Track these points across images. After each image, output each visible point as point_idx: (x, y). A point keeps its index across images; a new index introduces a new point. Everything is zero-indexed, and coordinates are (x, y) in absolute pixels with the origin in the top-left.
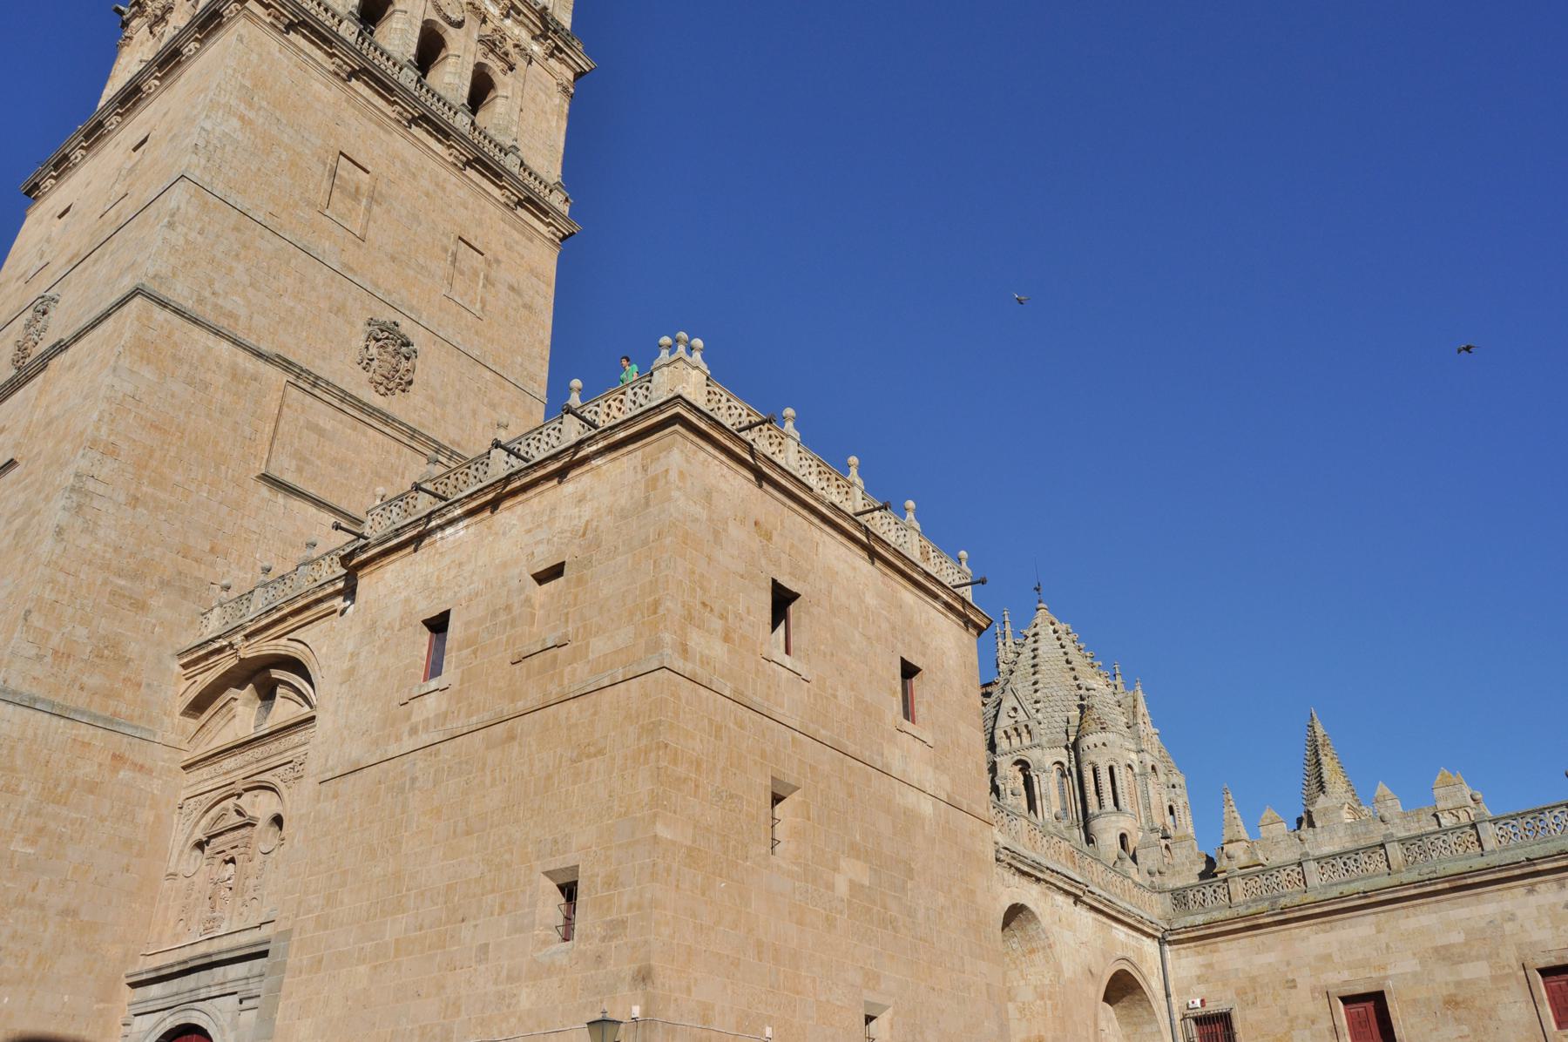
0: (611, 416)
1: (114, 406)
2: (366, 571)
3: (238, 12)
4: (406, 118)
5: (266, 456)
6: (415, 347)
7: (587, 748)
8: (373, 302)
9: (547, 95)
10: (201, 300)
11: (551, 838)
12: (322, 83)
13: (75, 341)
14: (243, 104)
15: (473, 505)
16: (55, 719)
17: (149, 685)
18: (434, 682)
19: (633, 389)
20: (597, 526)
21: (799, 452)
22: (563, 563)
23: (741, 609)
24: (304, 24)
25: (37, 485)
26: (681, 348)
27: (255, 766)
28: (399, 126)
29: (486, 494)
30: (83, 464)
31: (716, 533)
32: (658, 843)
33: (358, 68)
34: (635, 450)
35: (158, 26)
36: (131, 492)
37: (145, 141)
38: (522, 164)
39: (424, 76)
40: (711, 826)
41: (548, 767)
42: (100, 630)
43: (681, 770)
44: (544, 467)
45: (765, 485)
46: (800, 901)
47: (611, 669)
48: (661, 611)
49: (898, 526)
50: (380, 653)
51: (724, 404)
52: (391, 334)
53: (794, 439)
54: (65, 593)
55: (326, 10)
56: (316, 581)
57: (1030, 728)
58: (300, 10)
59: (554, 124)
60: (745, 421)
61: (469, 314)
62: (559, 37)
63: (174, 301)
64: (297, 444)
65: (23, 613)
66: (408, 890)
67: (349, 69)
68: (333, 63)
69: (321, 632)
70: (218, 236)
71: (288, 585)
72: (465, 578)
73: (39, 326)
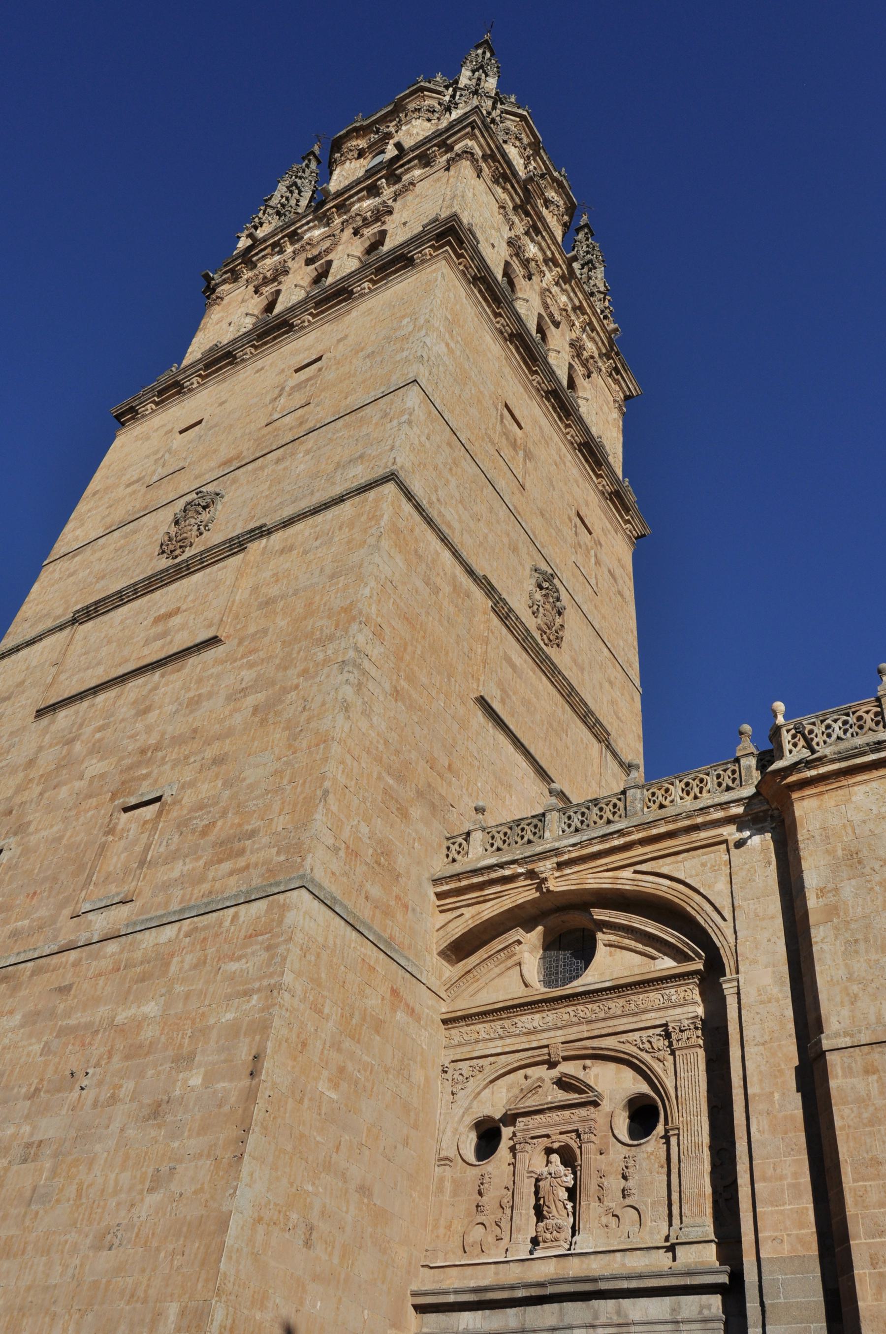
13: (284, 527)
17: (414, 910)
37: (319, 359)
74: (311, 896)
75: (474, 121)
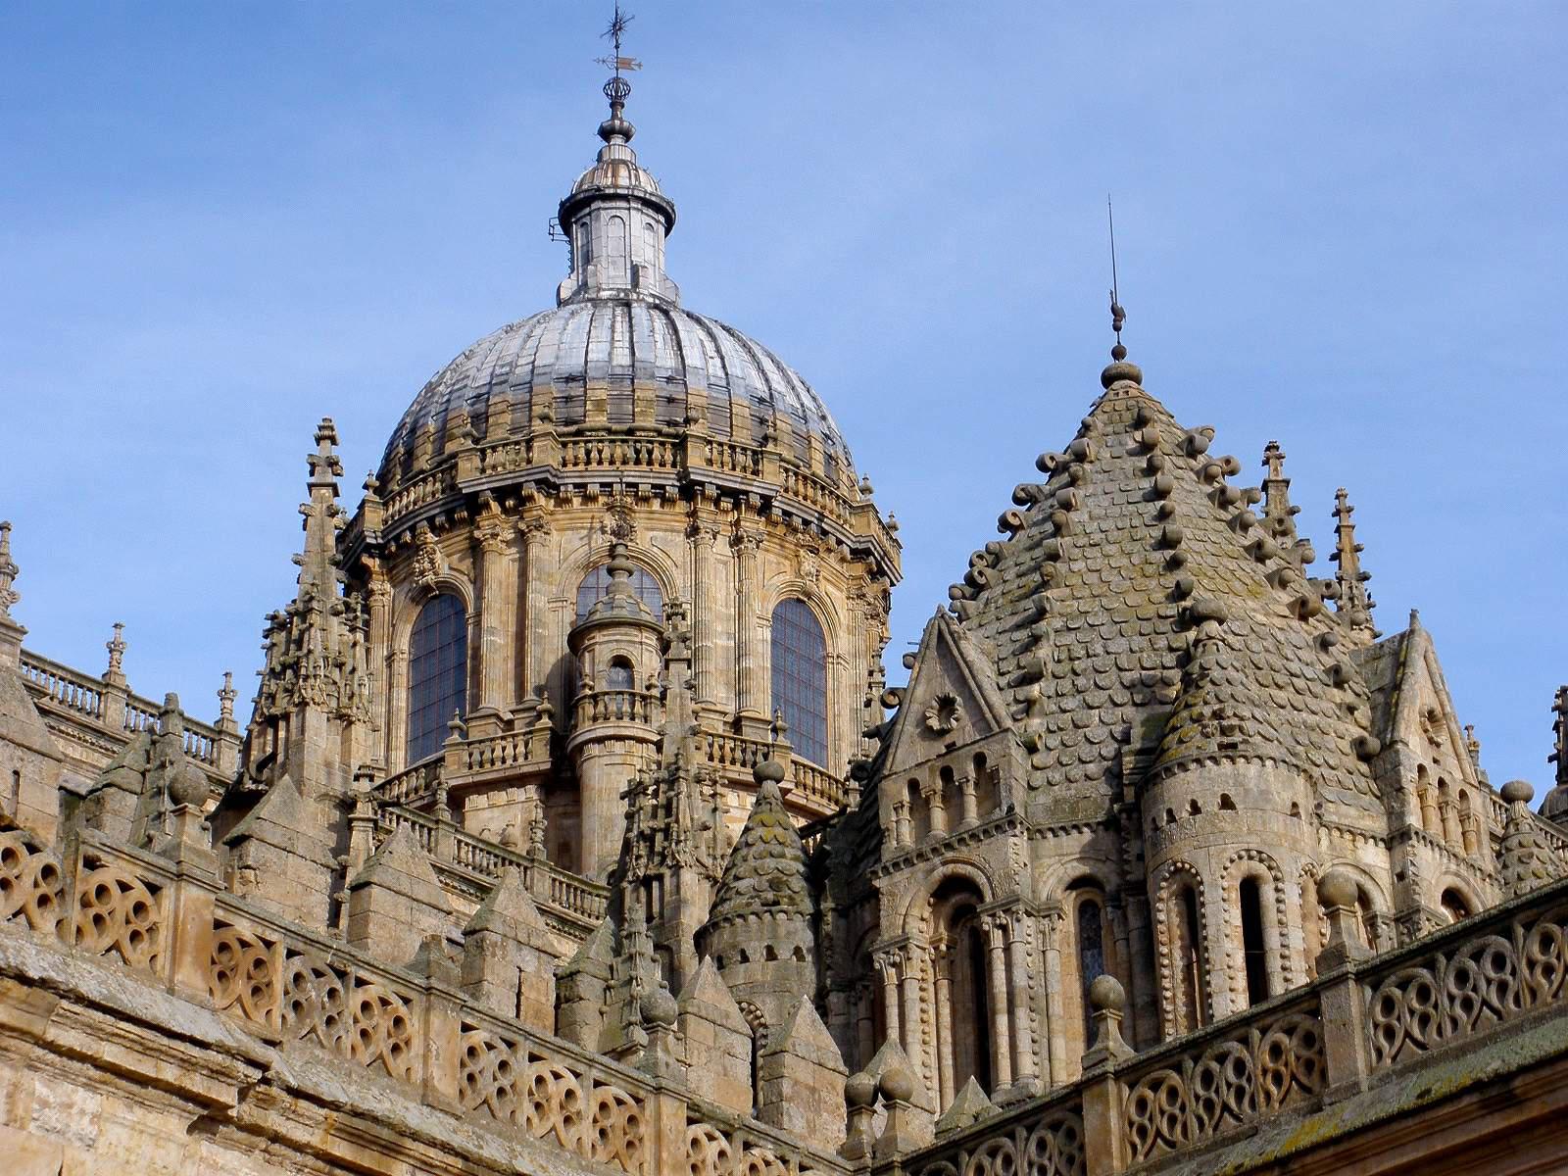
57: (990, 763)
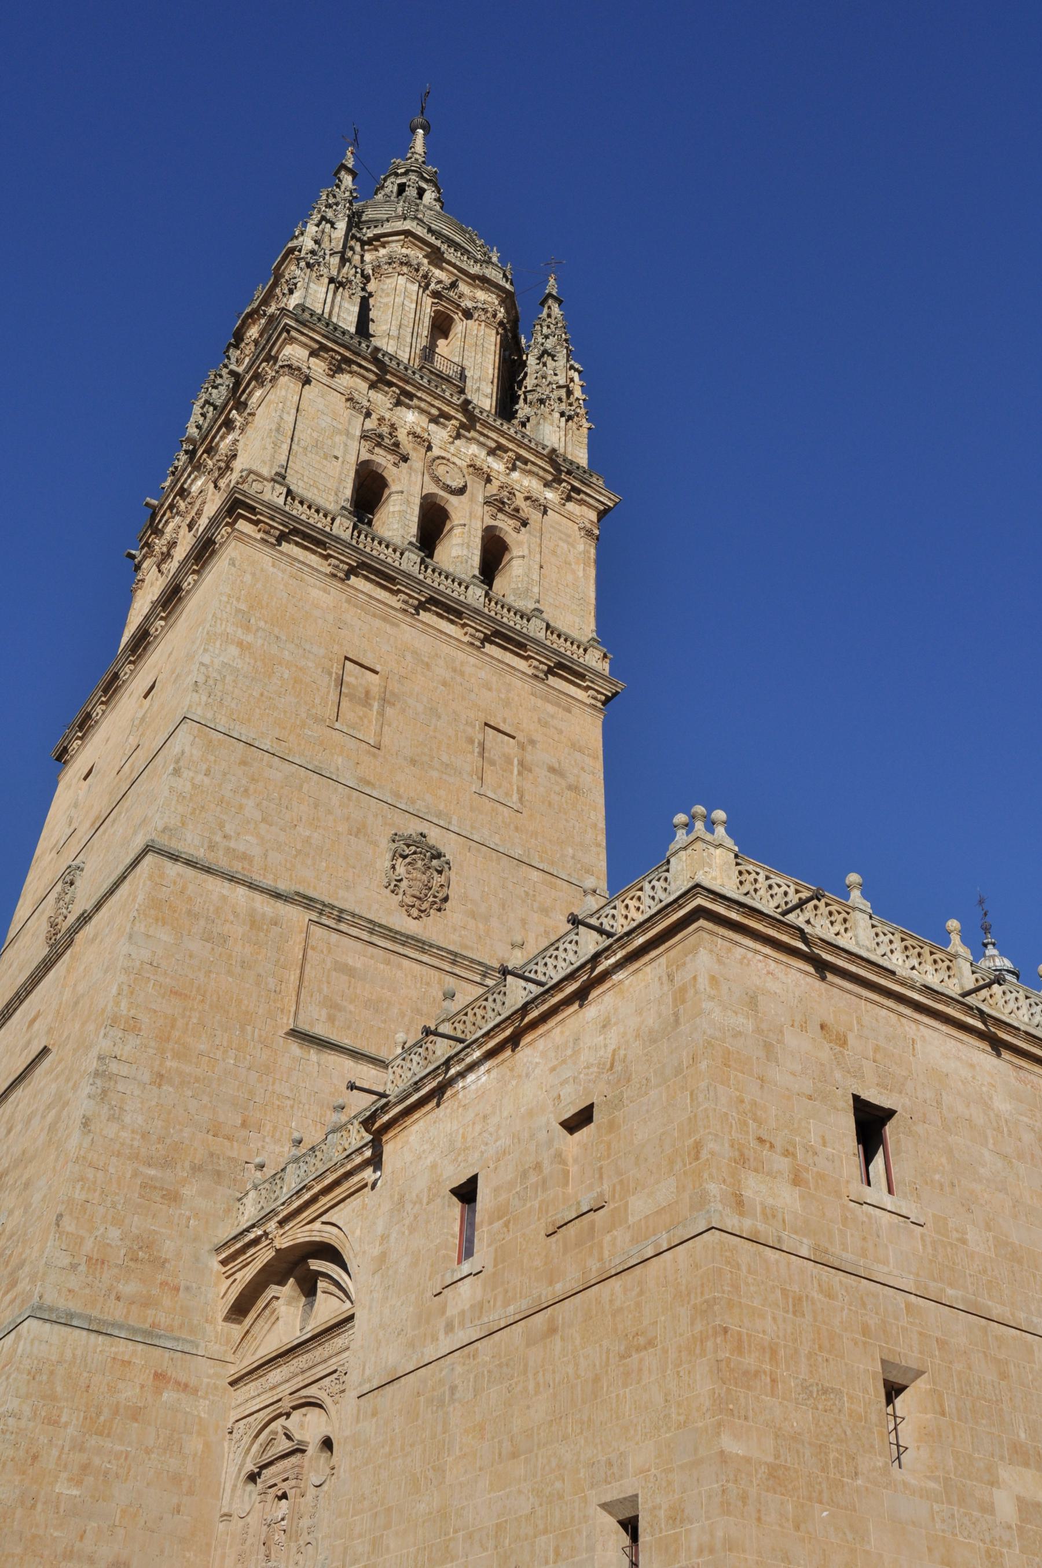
0: (629, 919)
1: (132, 976)
2: (391, 1134)
3: (229, 534)
4: (412, 606)
5: (293, 1009)
6: (447, 857)
7: (635, 1339)
8: (396, 815)
9: (568, 543)
10: (212, 847)
11: (604, 1459)
12: (319, 589)
13: (97, 910)
14: (240, 629)
15: (491, 1044)
16: (93, 1336)
17: (187, 1289)
18: (466, 1265)
19: (650, 882)
20: (625, 1056)
21: (873, 926)
22: (592, 1106)
23: (814, 1140)
24: (295, 531)
25: (67, 1072)
26: (699, 825)
27: (300, 1378)
28: (406, 616)
29: (504, 1030)
30: (104, 1045)
31: (768, 1047)
32: (726, 1462)
33: (355, 564)
34: (658, 956)
35: (165, 563)
36: (155, 1069)
37: (152, 687)
38: (548, 626)
39: (431, 556)
40: (799, 1434)
41: (595, 1366)
42: (133, 1229)
43: (750, 1361)
44: (561, 990)
45: (830, 977)
46: (943, 1531)
47: (655, 1235)
48: (704, 1155)
49: (1032, 1001)
50: (410, 1233)
51: (762, 883)
52: (418, 847)
53: (864, 912)
54: (95, 1191)
55: (317, 511)
56: (345, 1150)
58: (289, 519)
59: (581, 574)
60: (793, 899)
61: (505, 809)
62: (574, 477)
63: (185, 853)
64: (325, 989)
65: (55, 1218)
66: (456, 1531)
67: (346, 567)
68: (329, 565)
69: (353, 1211)
70: (225, 774)
71: (319, 1158)
72: (491, 1134)
73: (67, 898)
74: (41, 1322)
75: (286, 324)
